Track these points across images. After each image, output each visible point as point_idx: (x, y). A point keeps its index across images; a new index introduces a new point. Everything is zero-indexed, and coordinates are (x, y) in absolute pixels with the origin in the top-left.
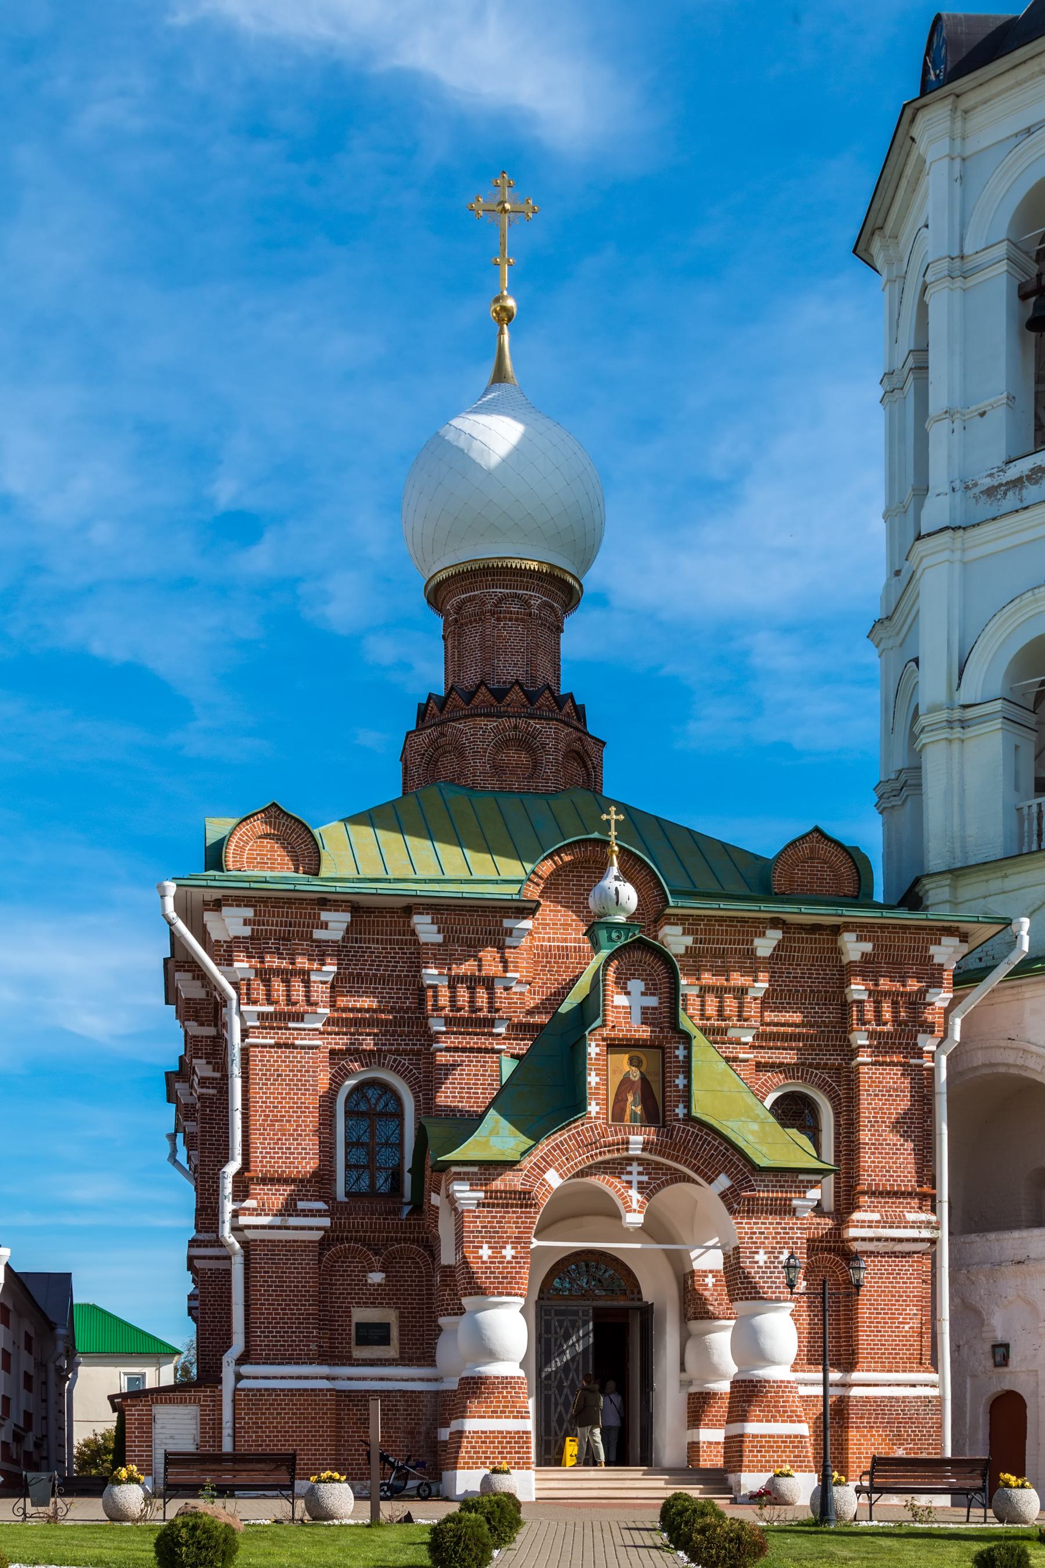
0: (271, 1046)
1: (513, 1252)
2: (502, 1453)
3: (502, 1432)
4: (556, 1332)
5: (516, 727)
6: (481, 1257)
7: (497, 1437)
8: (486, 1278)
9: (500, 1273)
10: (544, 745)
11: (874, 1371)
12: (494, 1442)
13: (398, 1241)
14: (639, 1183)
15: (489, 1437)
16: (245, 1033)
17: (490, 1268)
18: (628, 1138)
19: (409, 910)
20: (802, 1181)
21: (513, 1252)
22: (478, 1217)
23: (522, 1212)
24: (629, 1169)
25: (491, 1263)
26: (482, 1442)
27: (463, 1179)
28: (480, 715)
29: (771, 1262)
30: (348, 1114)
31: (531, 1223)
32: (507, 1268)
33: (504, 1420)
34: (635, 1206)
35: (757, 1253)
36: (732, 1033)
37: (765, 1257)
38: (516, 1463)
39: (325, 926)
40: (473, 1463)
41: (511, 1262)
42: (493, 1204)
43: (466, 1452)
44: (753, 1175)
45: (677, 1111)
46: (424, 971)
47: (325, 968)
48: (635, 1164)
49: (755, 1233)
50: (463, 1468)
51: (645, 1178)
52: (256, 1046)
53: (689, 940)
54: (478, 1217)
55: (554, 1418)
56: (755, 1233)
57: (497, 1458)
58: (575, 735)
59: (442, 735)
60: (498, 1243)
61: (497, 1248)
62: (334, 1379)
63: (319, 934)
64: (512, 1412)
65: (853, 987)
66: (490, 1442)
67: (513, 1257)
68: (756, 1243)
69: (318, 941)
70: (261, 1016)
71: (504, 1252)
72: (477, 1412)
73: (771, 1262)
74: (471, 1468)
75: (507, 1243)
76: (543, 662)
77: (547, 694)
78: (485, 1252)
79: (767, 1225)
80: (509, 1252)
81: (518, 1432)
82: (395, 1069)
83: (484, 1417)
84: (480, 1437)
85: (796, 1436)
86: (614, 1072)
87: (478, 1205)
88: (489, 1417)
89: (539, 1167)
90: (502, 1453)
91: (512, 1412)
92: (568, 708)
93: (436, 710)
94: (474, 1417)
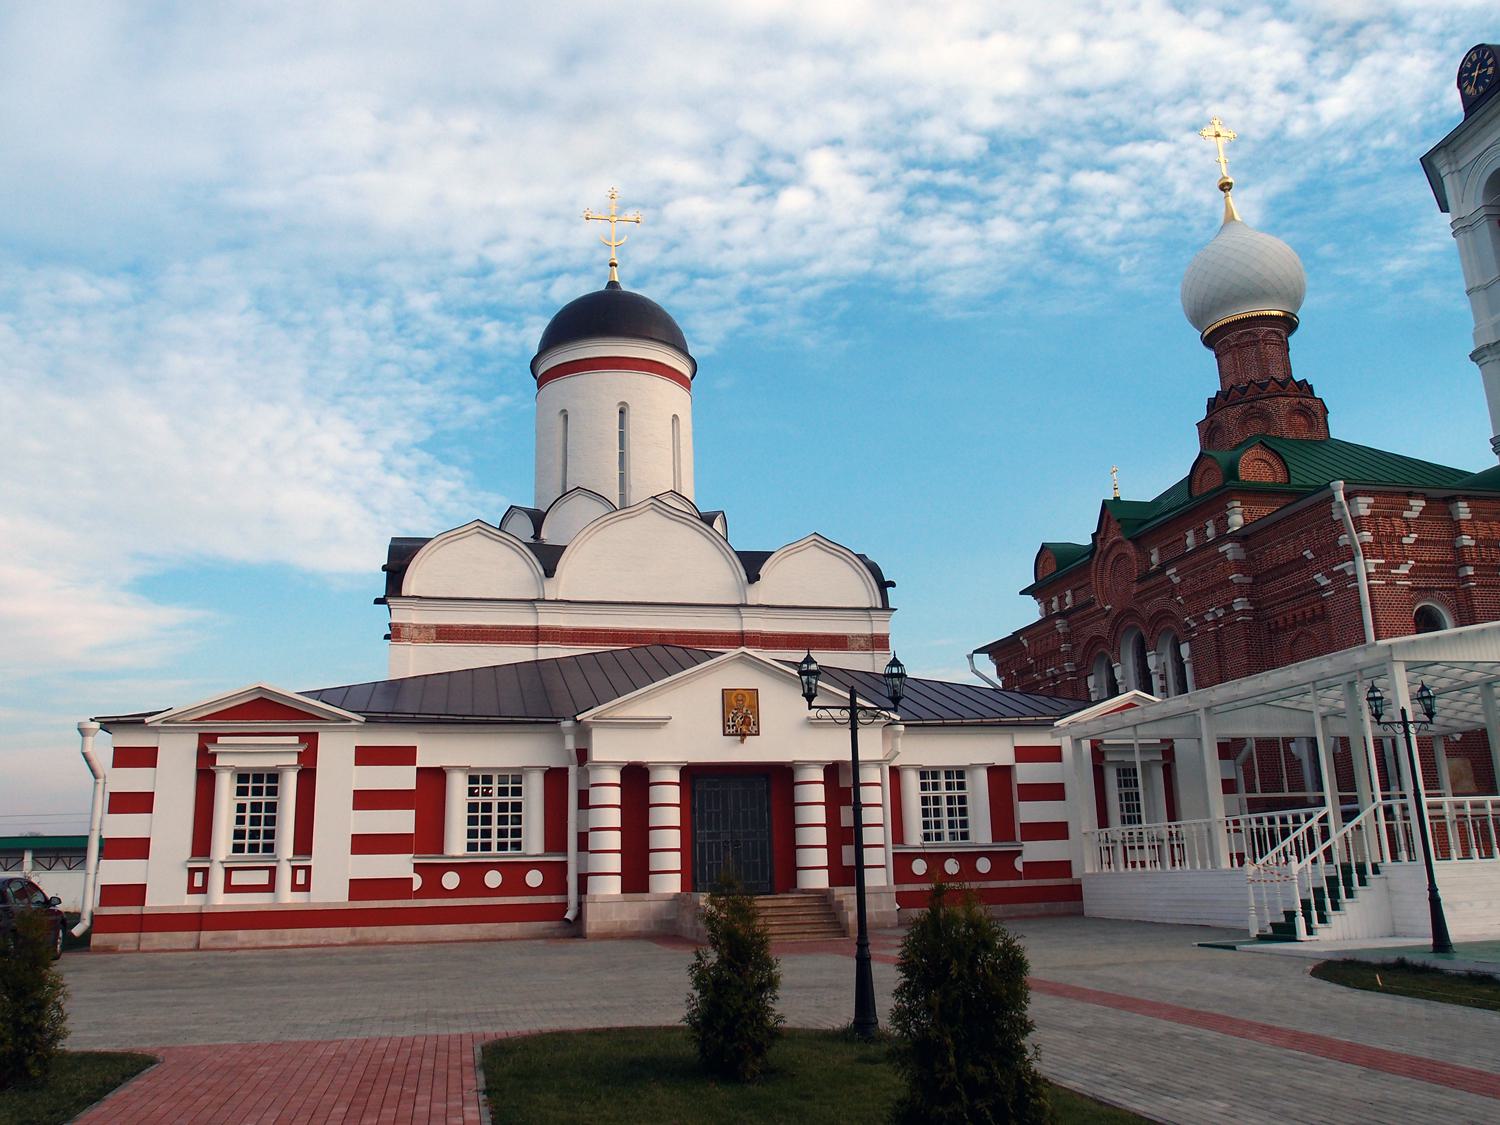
0: (1383, 585)
47: (1411, 535)
63: (1406, 514)
70: (1377, 566)
82: (1442, 601)
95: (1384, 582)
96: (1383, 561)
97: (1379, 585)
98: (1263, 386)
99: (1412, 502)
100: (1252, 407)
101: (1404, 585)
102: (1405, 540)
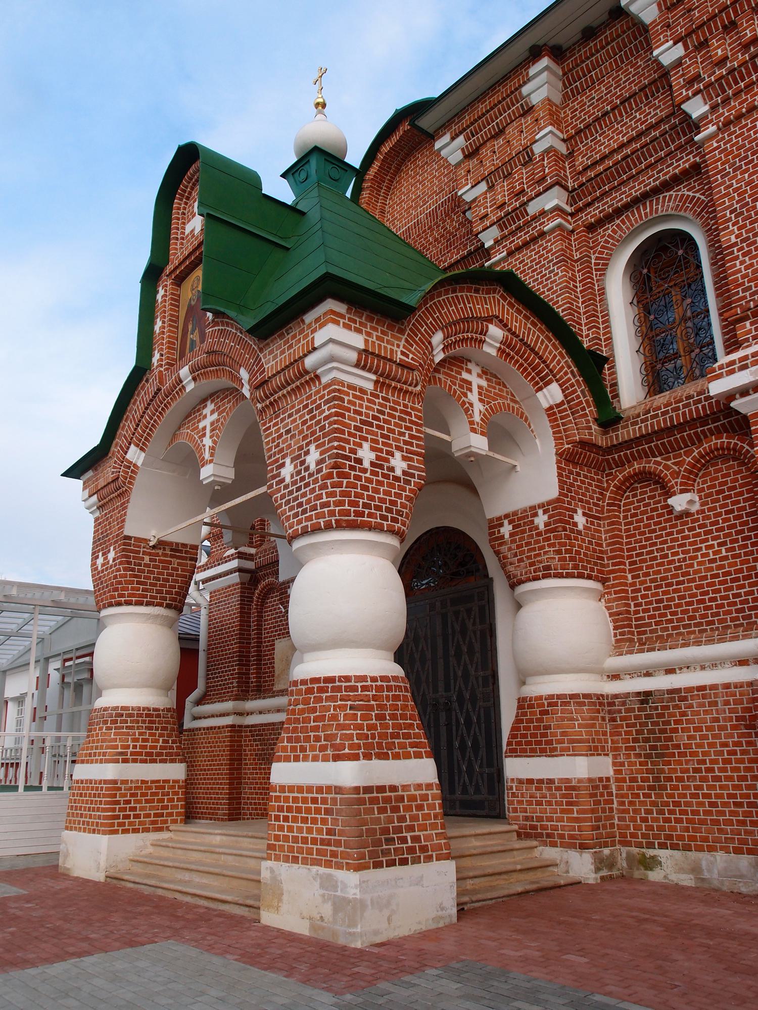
36: (533, 208)
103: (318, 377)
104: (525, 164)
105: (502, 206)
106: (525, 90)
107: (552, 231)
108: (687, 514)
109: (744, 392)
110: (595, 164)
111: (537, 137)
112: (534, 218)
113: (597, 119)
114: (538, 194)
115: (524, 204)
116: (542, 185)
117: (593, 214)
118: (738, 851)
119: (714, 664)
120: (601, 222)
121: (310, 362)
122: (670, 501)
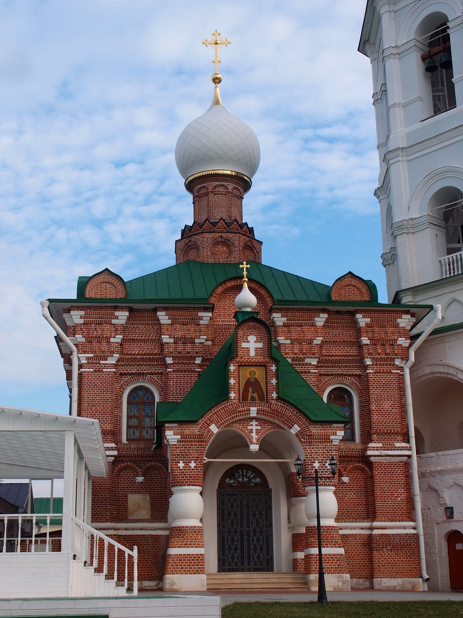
0: (92, 372)
1: (195, 464)
2: (190, 565)
3: (189, 555)
4: (227, 505)
5: (221, 236)
6: (179, 467)
7: (187, 557)
8: (182, 477)
9: (188, 475)
10: (233, 244)
11: (384, 521)
12: (185, 560)
13: (151, 461)
14: (256, 430)
15: (183, 558)
16: (80, 366)
17: (183, 472)
18: (249, 409)
19: (155, 310)
20: (334, 427)
21: (195, 464)
22: (178, 448)
23: (199, 445)
24: (251, 423)
25: (184, 470)
26: (180, 560)
27: (170, 430)
28: (205, 232)
29: (322, 467)
30: (129, 403)
31: (203, 450)
32: (192, 472)
33: (190, 549)
34: (254, 441)
35: (314, 462)
36: (307, 361)
37: (318, 465)
38: (196, 571)
39: (117, 318)
40: (175, 571)
41: (193, 469)
42: (185, 441)
43: (172, 565)
44: (310, 425)
45: (273, 395)
46: (163, 336)
48: (254, 421)
49: (313, 453)
50: (170, 574)
51: (259, 428)
52: (85, 372)
53: (285, 319)
54: (178, 448)
55: (227, 547)
56: (313, 453)
57: (187, 568)
58: (248, 239)
59: (190, 241)
60: (188, 460)
61: (187, 463)
62: (118, 529)
63: (114, 321)
64: (195, 544)
65: (362, 338)
66: (184, 560)
67: (195, 467)
68: (313, 458)
69: (115, 325)
70: (88, 358)
71: (190, 464)
72: (177, 544)
73: (322, 467)
74: (174, 574)
75: (192, 460)
76: (234, 210)
77: (235, 223)
78: (181, 465)
79: (318, 449)
80: (193, 465)
81: (198, 555)
82: (151, 381)
83: (180, 547)
84: (179, 558)
85: (338, 555)
86: (243, 378)
87: (178, 441)
88: (183, 547)
89: (207, 424)
90: (190, 565)
91: (195, 544)
92: (245, 228)
93: (188, 232)
94: (175, 547)
95: (92, 370)
96: (92, 355)
97: (89, 372)
98: (228, 225)
99: (117, 313)
100: (190, 241)
101: (110, 372)
102: (112, 340)
103: (332, 442)
104: (308, 344)
105: (296, 354)
106: (316, 319)
107: (313, 373)
108: (345, 483)
109: (375, 456)
110: (329, 356)
111: (317, 338)
112: (306, 364)
113: (334, 341)
114: (311, 358)
115: (305, 358)
116: (313, 355)
117: (323, 371)
118: (359, 578)
119: (354, 528)
120: (324, 375)
121: (332, 437)
122: (342, 478)
